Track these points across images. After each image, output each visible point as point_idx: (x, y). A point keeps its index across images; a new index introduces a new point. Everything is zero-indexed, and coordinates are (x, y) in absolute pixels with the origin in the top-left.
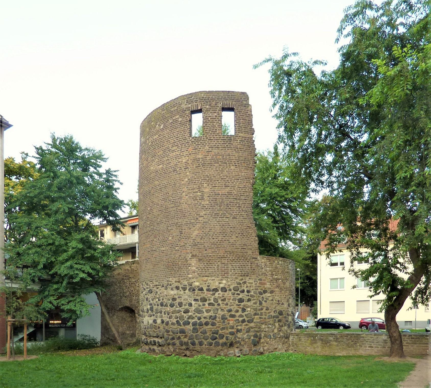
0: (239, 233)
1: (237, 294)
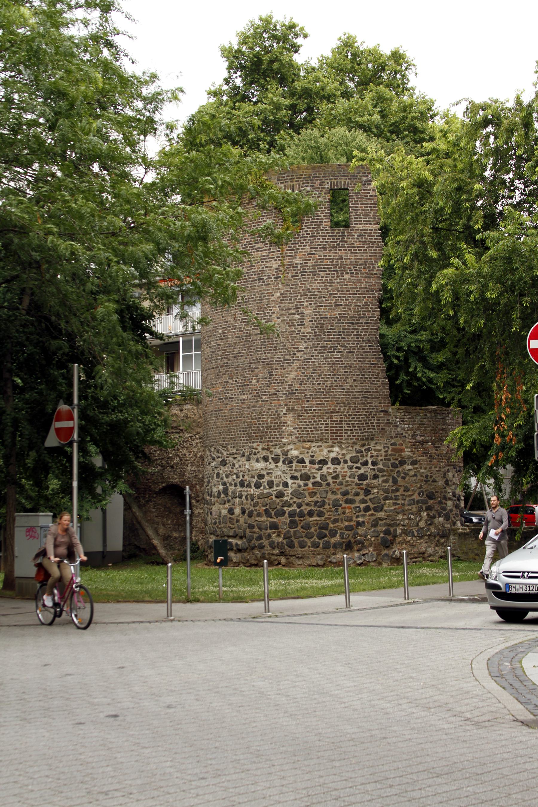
0: (359, 375)
1: (356, 468)
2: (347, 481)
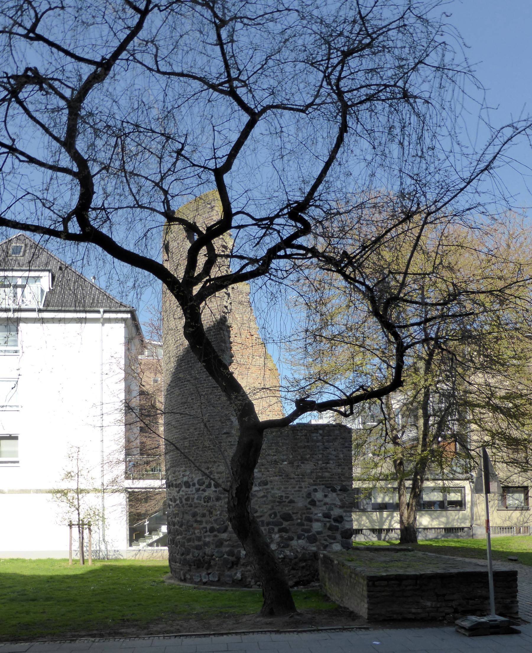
2: (195, 503)
